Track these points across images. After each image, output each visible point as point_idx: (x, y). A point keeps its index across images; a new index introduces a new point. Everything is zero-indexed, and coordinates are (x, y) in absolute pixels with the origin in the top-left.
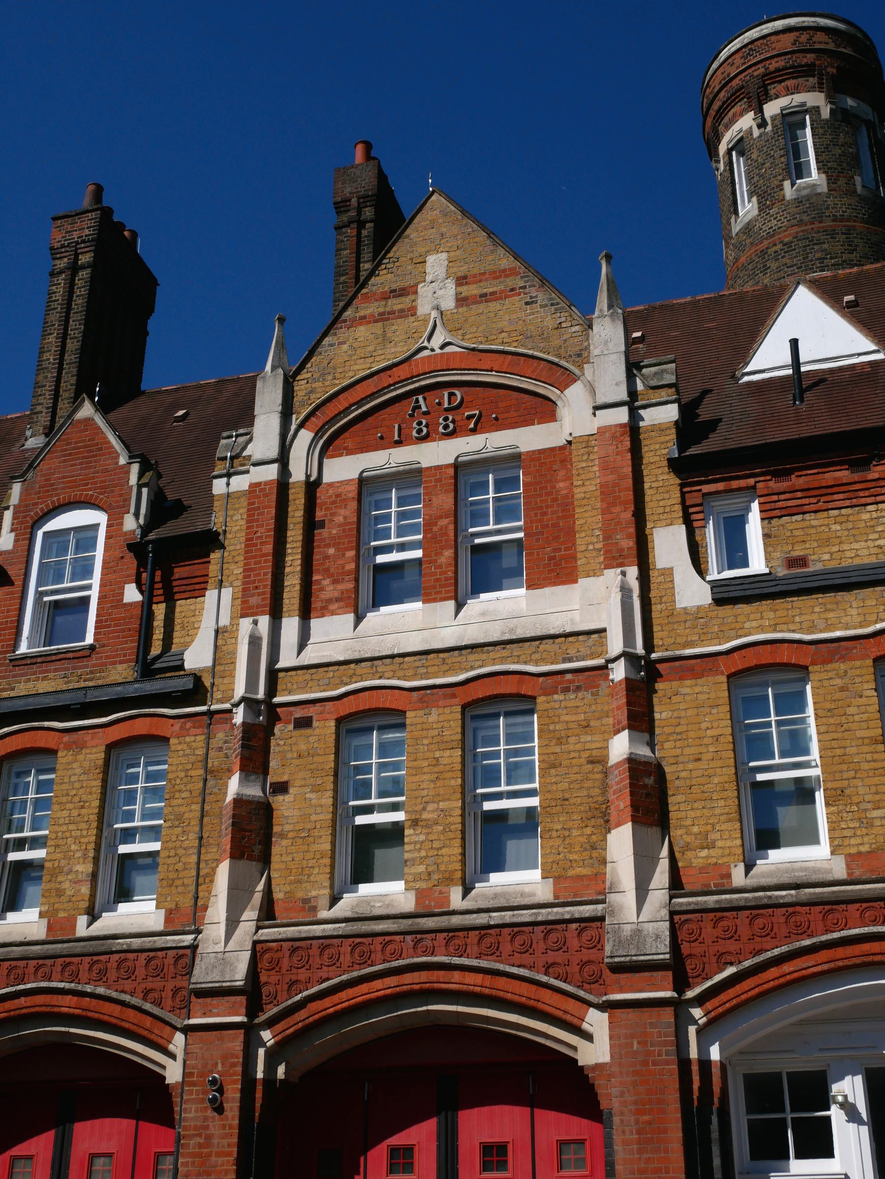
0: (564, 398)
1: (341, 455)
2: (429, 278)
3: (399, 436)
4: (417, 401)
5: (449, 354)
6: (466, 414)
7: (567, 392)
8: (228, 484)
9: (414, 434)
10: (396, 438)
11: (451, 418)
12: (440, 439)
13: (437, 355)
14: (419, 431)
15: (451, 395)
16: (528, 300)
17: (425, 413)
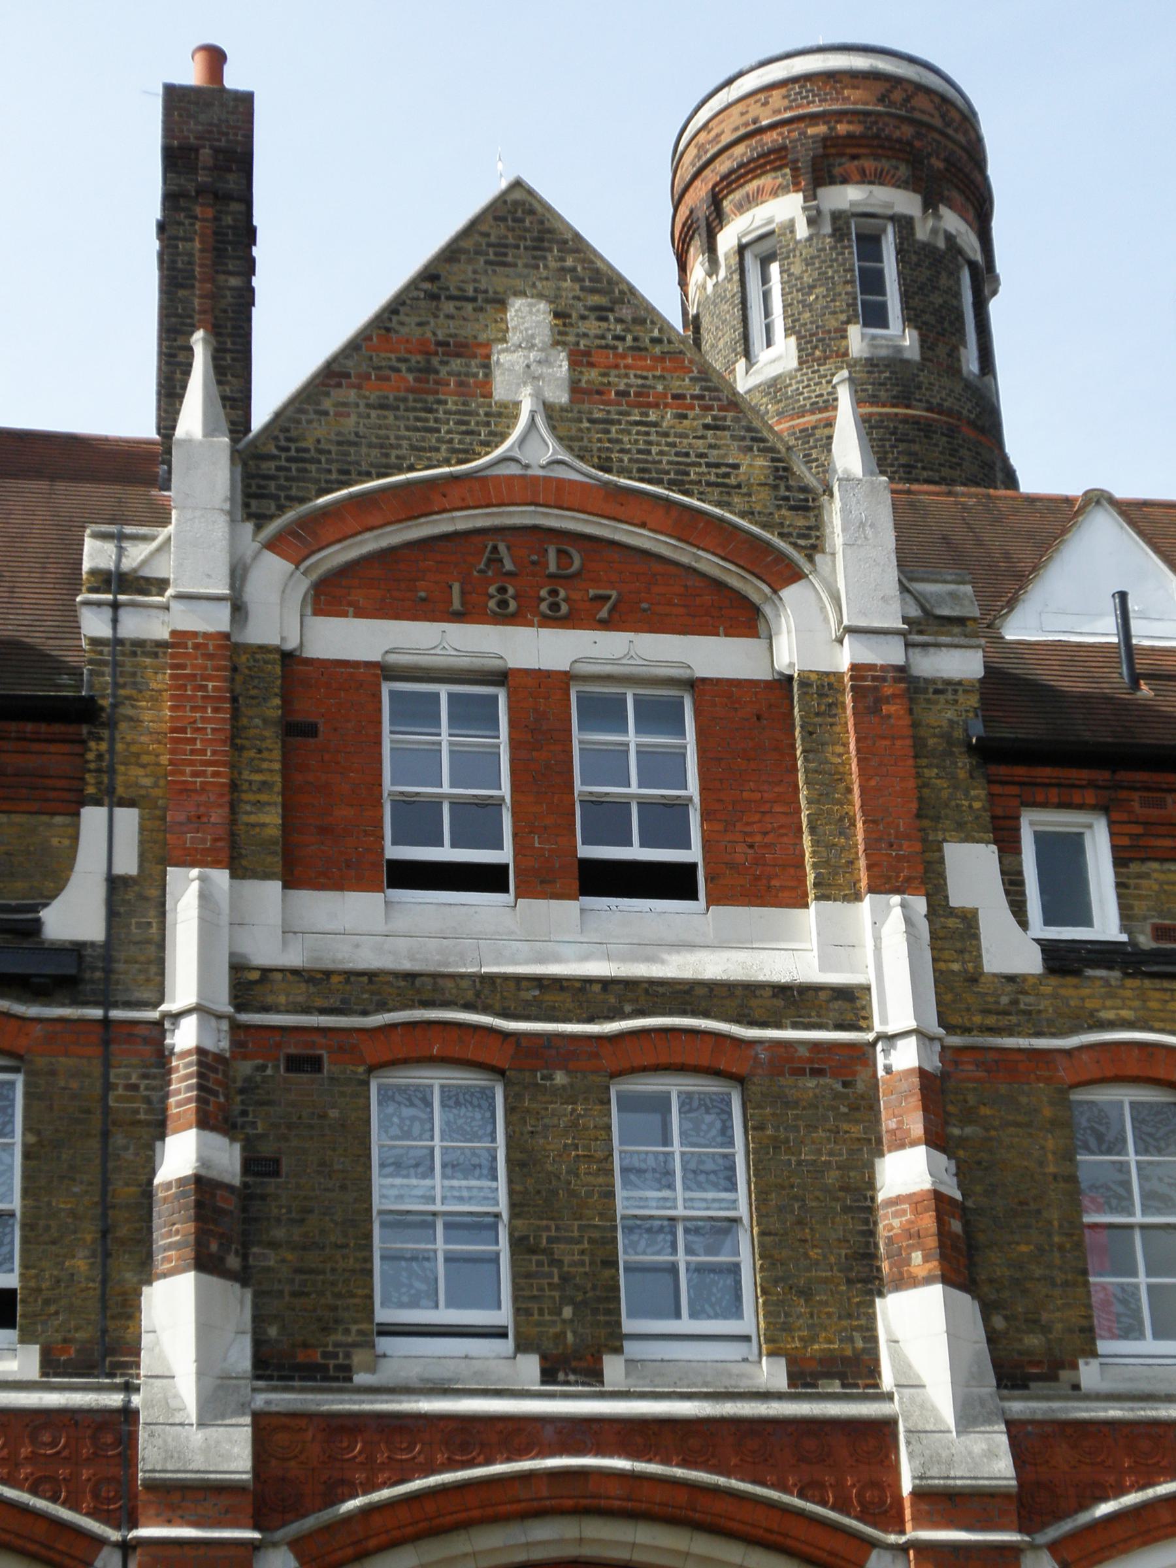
0: (777, 602)
1: (344, 614)
2: (514, 338)
3: (463, 604)
4: (495, 549)
5: (560, 482)
6: (592, 592)
7: (785, 593)
8: (115, 621)
9: (492, 604)
10: (457, 605)
11: (562, 593)
12: (541, 625)
13: (535, 479)
14: (503, 604)
15: (560, 552)
16: (709, 420)
17: (509, 574)
